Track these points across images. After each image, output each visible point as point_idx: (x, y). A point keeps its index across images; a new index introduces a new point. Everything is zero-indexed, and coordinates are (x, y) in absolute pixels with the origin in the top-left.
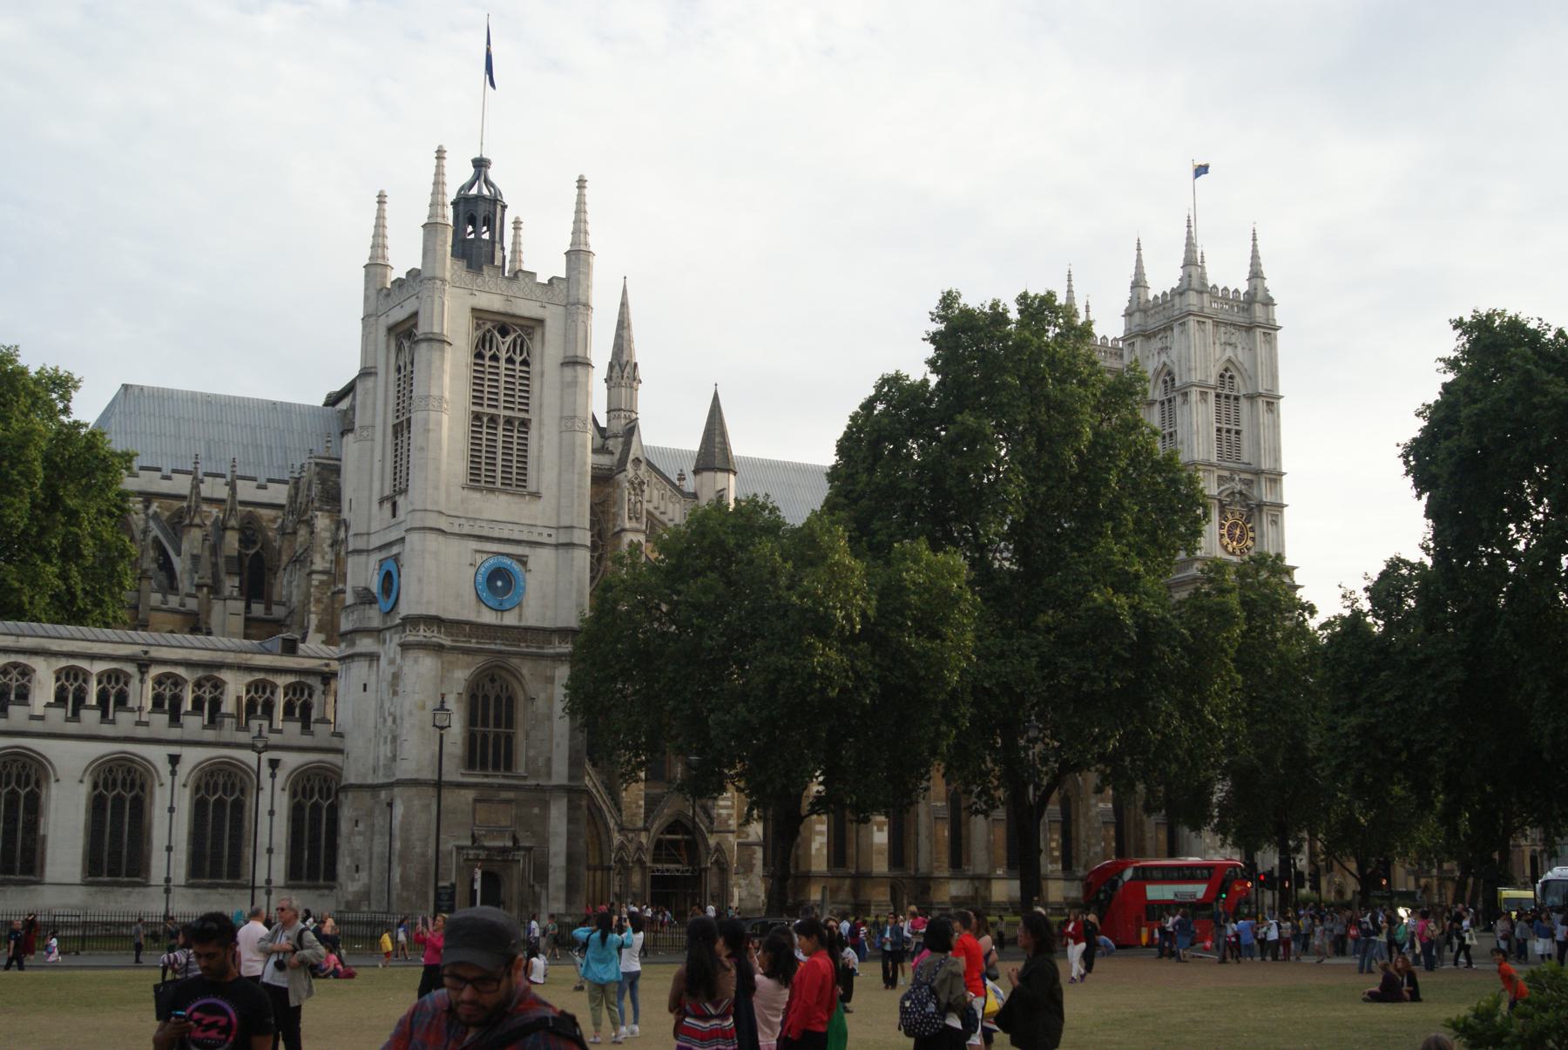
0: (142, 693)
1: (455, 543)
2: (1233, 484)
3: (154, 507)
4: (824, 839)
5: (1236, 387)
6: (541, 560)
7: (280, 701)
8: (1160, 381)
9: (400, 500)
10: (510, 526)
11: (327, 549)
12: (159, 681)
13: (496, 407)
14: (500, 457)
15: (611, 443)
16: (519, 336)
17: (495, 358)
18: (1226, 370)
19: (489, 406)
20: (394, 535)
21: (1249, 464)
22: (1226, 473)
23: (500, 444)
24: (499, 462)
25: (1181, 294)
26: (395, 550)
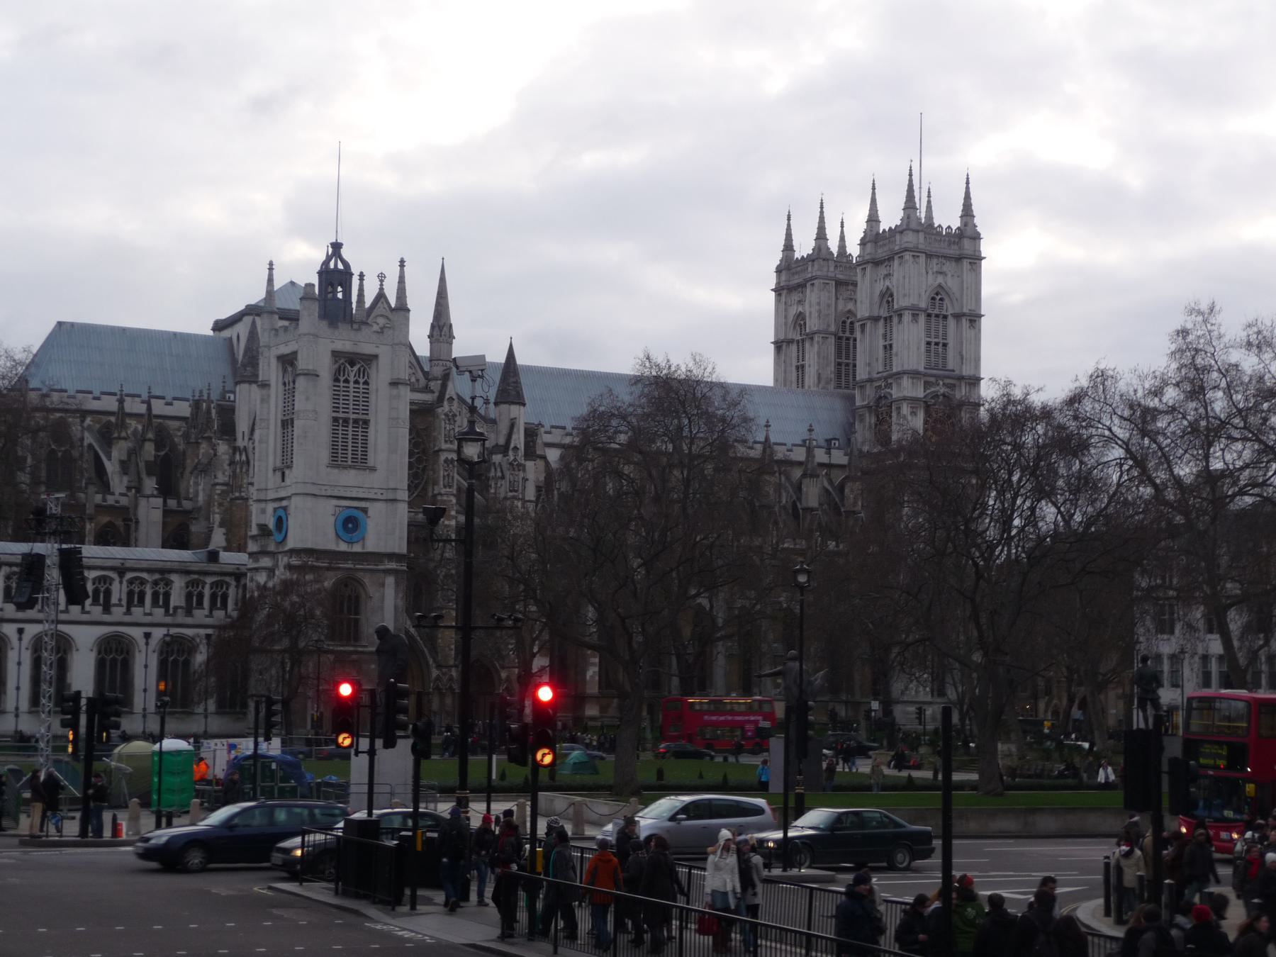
0: (118, 591)
1: (322, 502)
2: (938, 388)
3: (88, 421)
4: (596, 669)
5: (945, 308)
6: (375, 510)
7: (207, 592)
8: (885, 300)
9: (287, 472)
10: (357, 489)
11: (227, 467)
12: (131, 582)
13: (348, 413)
14: (350, 444)
15: (432, 384)
16: (363, 366)
17: (347, 381)
18: (937, 294)
19: (343, 412)
20: (282, 494)
21: (953, 371)
22: (933, 379)
23: (350, 437)
24: (350, 448)
25: (901, 232)
26: (284, 503)
